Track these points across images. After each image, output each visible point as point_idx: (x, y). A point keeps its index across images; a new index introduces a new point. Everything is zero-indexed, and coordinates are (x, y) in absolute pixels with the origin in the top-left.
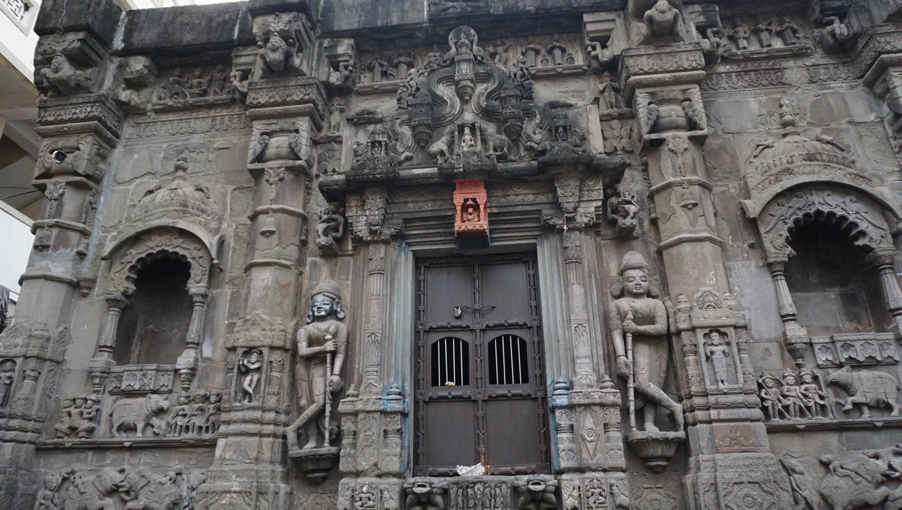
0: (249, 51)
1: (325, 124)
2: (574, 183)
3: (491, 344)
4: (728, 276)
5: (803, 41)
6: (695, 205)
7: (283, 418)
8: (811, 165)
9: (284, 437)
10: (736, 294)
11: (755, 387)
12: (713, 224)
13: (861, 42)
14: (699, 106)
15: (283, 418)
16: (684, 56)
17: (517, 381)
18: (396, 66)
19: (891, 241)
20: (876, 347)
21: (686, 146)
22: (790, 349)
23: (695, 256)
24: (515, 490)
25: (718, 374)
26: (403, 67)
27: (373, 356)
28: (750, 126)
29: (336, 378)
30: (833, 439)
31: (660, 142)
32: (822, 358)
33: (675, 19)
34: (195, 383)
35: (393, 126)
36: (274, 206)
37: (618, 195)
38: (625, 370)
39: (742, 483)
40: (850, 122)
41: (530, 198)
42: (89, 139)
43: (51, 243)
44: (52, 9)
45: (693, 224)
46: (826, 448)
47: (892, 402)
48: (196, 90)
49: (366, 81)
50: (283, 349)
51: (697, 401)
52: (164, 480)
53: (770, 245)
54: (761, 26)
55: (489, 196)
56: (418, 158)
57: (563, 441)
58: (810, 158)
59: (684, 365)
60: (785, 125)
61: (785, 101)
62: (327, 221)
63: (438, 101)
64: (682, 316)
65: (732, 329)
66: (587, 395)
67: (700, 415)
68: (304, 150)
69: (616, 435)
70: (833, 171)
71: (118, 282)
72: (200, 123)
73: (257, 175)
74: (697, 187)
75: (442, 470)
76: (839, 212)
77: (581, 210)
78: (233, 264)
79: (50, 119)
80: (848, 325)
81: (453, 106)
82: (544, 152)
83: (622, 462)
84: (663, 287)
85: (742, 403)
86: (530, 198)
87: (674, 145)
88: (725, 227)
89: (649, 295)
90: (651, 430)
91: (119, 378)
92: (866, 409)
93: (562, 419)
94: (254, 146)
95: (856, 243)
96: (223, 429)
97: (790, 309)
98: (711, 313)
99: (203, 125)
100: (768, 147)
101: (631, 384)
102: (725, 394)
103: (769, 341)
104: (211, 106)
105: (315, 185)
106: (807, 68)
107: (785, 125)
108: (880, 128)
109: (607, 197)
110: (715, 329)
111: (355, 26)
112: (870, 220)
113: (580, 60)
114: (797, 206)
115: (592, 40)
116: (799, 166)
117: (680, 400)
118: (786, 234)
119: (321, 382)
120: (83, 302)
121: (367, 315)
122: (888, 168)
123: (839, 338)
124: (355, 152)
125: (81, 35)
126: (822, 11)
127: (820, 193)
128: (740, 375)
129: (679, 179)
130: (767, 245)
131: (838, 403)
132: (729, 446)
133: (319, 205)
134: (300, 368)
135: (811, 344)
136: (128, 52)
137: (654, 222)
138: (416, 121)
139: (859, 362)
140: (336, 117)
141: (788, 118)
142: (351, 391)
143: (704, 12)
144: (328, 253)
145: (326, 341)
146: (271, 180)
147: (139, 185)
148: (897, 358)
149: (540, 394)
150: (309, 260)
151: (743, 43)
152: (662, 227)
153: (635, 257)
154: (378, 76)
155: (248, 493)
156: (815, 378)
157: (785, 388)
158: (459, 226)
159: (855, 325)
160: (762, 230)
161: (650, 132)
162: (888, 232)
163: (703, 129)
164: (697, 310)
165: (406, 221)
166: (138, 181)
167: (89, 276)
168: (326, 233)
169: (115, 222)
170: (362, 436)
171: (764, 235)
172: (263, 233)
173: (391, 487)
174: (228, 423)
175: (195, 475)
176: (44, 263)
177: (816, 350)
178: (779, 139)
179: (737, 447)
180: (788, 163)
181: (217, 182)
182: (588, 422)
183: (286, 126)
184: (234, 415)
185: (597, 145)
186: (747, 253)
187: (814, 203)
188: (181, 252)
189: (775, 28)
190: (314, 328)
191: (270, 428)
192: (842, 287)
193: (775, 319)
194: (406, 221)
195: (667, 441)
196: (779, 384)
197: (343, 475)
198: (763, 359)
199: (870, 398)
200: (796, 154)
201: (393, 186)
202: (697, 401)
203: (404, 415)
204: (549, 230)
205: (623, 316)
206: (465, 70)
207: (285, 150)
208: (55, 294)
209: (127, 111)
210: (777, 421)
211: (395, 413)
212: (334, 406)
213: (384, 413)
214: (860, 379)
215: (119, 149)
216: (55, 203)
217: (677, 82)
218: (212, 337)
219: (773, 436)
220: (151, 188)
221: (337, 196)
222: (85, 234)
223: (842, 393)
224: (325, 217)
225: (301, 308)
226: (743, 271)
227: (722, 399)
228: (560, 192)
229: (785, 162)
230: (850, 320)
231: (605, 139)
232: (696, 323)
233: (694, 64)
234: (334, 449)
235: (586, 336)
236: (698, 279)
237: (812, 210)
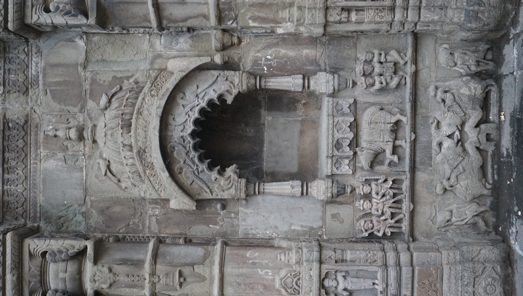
6: (181, 274)
8: (136, 128)
12: (199, 251)
19: (233, 72)
20: (341, 119)
21: (106, 270)
23: (239, 284)
25: (366, 287)
28: (78, 174)
30: (421, 176)
32: (345, 168)
39: (474, 292)
40: (85, 68)
45: (201, 279)
47: (394, 120)
53: (226, 192)
58: (127, 126)
60: (81, 138)
65: (324, 266)
70: (146, 106)
74: (158, 267)
76: (195, 115)
80: (301, 111)
85: (397, 273)
87: (104, 283)
92: (398, 143)
95: (229, 102)
97: (298, 190)
98: (305, 284)
100: (108, 167)
102: (387, 285)
103: (324, 212)
107: (81, 138)
108: (96, 38)
112: (206, 86)
114: (184, 154)
116: (137, 141)
118: (214, 175)
122: (145, 46)
123: (330, 152)
127: (171, 128)
129: (147, 285)
130: (225, 195)
131: (390, 164)
132: (436, 292)
135: (332, 176)
139: (353, 138)
141: (73, 134)
148: (352, 101)
156: (368, 182)
157: (374, 212)
159: (300, 106)
160: (209, 196)
162: (222, 73)
163: (86, 247)
171: (214, 196)
177: (338, 172)
178: (98, 147)
179: (438, 285)
180: (131, 150)
186: (230, 213)
187: (182, 137)
192: (261, 107)
193: (303, 203)
198: (342, 222)
199: (388, 137)
200: (120, 139)
210: (405, 226)
214: (370, 142)
217: (18, 265)
223: (380, 157)
226: (250, 221)
229: (129, 153)
230: (295, 109)
236: (265, 287)
237: (190, 142)
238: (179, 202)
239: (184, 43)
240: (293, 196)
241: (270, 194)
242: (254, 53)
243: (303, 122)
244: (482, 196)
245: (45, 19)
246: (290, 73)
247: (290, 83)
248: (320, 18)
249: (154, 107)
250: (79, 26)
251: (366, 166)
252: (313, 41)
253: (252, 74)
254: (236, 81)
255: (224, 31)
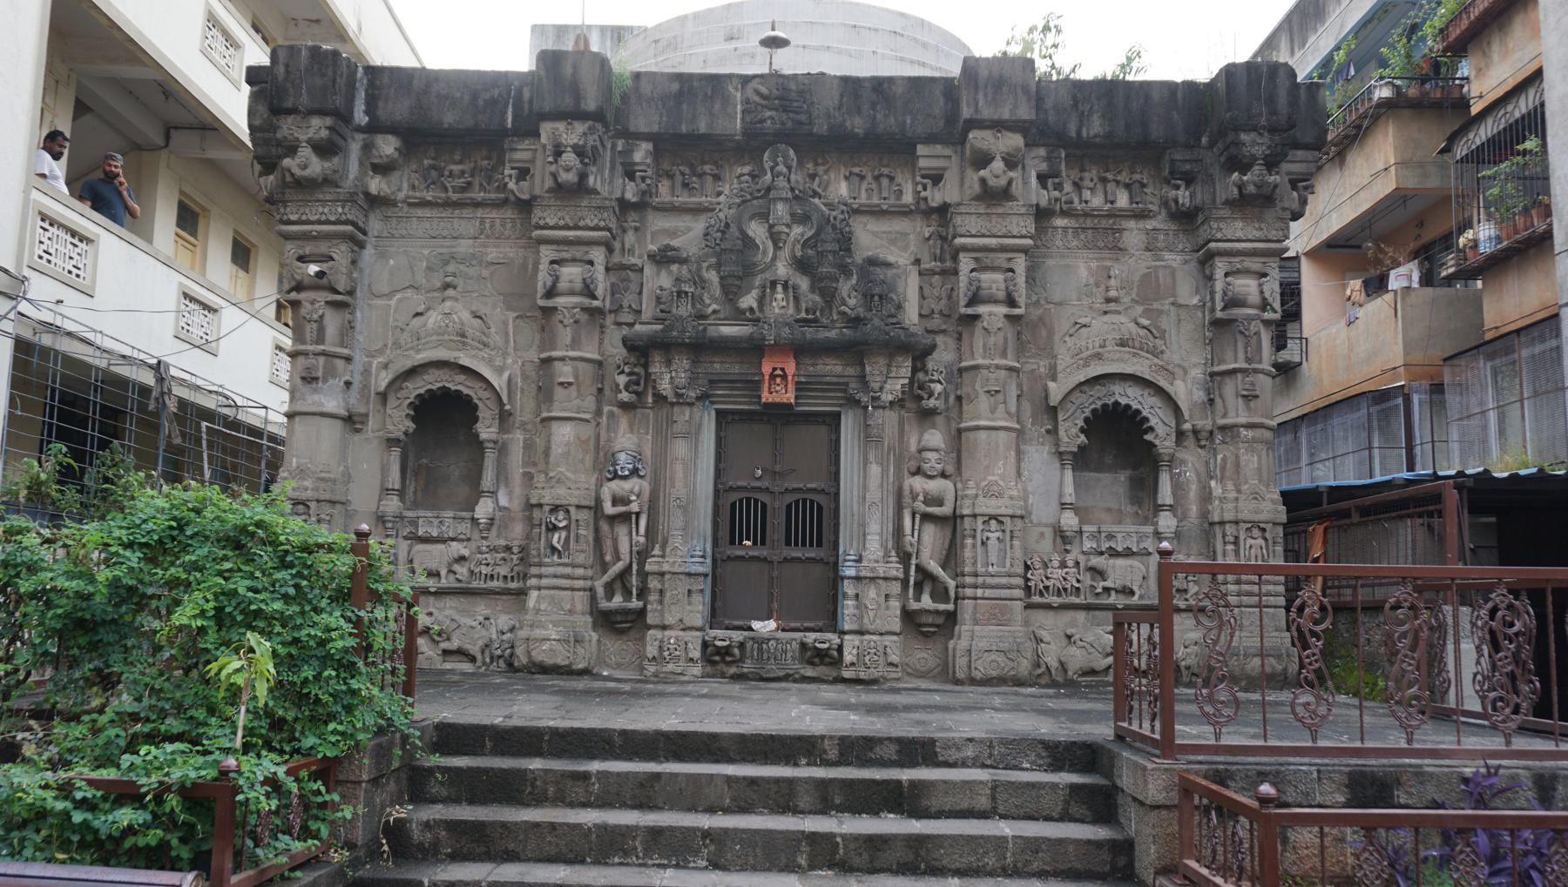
0: (526, 144)
1: (617, 245)
2: (882, 361)
3: (789, 507)
4: (1019, 460)
5: (1149, 198)
7: (590, 572)
9: (591, 589)
10: (1024, 483)
11: (1020, 570)
12: (1013, 409)
13: (1200, 219)
14: (1021, 279)
15: (590, 572)
16: (1015, 219)
17: (811, 545)
18: (701, 176)
22: (1062, 538)
24: (803, 645)
26: (709, 178)
27: (677, 521)
29: (642, 540)
30: (1081, 616)
31: (976, 317)
32: (1088, 545)
33: (1010, 182)
34: (494, 532)
35: (699, 269)
36: (572, 354)
37: (926, 372)
38: (909, 549)
41: (839, 369)
42: (344, 247)
43: (320, 374)
44: (286, 79)
46: (1073, 624)
47: (1135, 588)
48: (460, 182)
49: (664, 193)
50: (589, 508)
51: (968, 580)
52: (474, 624)
54: (1109, 176)
55: (797, 364)
56: (726, 311)
57: (848, 607)
58: (1122, 343)
59: (963, 546)
60: (1108, 300)
61: (1115, 271)
62: (630, 374)
63: (748, 243)
64: (967, 502)
66: (873, 570)
67: (969, 592)
68: (601, 288)
69: (895, 605)
71: (399, 421)
72: (465, 224)
73: (548, 312)
75: (736, 623)
76: (1135, 406)
77: (887, 386)
78: (524, 407)
79: (294, 217)
80: (1130, 509)
81: (765, 252)
82: (854, 322)
83: (897, 627)
84: (955, 470)
86: (839, 369)
88: (1027, 407)
89: (943, 475)
90: (926, 601)
91: (414, 523)
93: (849, 588)
94: (543, 278)
96: (533, 582)
97: (1068, 500)
98: (993, 502)
99: (470, 228)
101: (914, 562)
103: (1046, 525)
104: (477, 205)
105: (610, 319)
106: (1147, 232)
107: (1108, 300)
108: (1200, 314)
109: (915, 371)
110: (992, 517)
111: (655, 128)
113: (908, 198)
115: (923, 177)
117: (955, 576)
118: (1081, 423)
119: (626, 541)
120: (357, 437)
121: (672, 479)
124: (658, 298)
125: (329, 121)
126: (1171, 173)
128: (1008, 562)
129: (987, 362)
130: (1062, 433)
133: (617, 352)
134: (605, 527)
136: (374, 128)
137: (959, 399)
138: (726, 269)
140: (630, 238)
141: (1113, 293)
142: (656, 551)
143: (1048, 159)
144: (625, 406)
145: (630, 502)
146: (566, 322)
147: (400, 300)
149: (832, 559)
150: (606, 409)
151: (1087, 194)
152: (965, 407)
153: (935, 437)
154: (679, 190)
155: (567, 641)
156: (1077, 564)
158: (766, 397)
159: (1135, 508)
160: (1060, 417)
161: (967, 306)
164: (981, 498)
165: (711, 382)
166: (398, 296)
167: (362, 410)
168: (627, 388)
169: (380, 345)
170: (668, 594)
172: (561, 384)
173: (694, 642)
174: (540, 576)
175: (504, 621)
176: (316, 397)
181: (494, 307)
182: (872, 593)
183: (578, 255)
184: (544, 570)
185: (911, 315)
188: (466, 391)
189: (1124, 177)
190: (616, 486)
191: (580, 583)
193: (1055, 505)
194: (711, 382)
195: (937, 612)
196: (1046, 566)
197: (649, 627)
199: (1118, 584)
201: (702, 348)
202: (968, 580)
203: (706, 575)
204: (853, 402)
205: (914, 497)
206: (781, 209)
207: (578, 286)
208: (331, 432)
209: (375, 202)
210: (1037, 599)
211: (699, 575)
212: (641, 564)
213: (689, 575)
215: (368, 254)
216: (315, 326)
218: (507, 485)
219: (1028, 611)
220: (421, 309)
221: (641, 350)
222: (348, 359)
224: (627, 370)
225: (607, 468)
227: (989, 580)
228: (868, 369)
231: (922, 297)
232: (977, 511)
233: (1024, 232)
234: (641, 604)
235: (879, 514)
236: (987, 467)
238: (1056, 391)
239: (1200, 395)
240: (1061, 496)
241: (1062, 475)
242: (1191, 461)
243: (1120, 511)
244: (1066, 671)
245: (1219, 274)
246: (1174, 494)
247: (1165, 494)
248: (1228, 516)
249: (1140, 366)
250: (1213, 299)
251: (1090, 564)
252: (1204, 514)
253: (1172, 459)
254: (1167, 443)
255: (1211, 432)
